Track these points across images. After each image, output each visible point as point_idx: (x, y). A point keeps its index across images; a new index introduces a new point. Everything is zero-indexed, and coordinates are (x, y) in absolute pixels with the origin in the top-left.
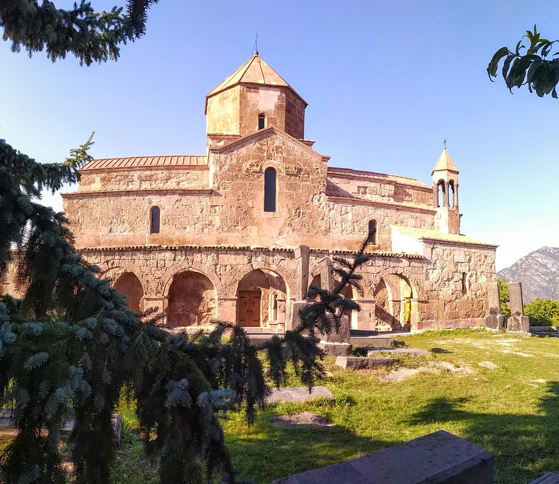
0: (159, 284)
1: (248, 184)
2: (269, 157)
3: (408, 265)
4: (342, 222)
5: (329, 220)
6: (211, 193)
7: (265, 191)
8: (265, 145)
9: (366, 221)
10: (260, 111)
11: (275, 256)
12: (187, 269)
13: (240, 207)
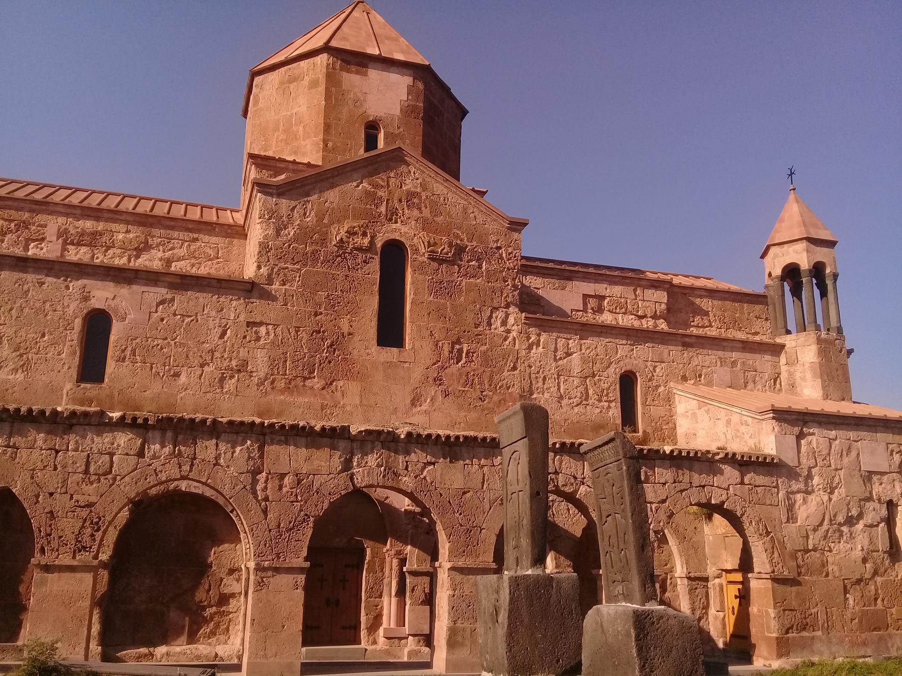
0: (87, 524)
1: (341, 278)
3: (739, 480)
4: (559, 376)
5: (528, 371)
9: (613, 374)
10: (368, 116)
12: (172, 487)
13: (319, 332)
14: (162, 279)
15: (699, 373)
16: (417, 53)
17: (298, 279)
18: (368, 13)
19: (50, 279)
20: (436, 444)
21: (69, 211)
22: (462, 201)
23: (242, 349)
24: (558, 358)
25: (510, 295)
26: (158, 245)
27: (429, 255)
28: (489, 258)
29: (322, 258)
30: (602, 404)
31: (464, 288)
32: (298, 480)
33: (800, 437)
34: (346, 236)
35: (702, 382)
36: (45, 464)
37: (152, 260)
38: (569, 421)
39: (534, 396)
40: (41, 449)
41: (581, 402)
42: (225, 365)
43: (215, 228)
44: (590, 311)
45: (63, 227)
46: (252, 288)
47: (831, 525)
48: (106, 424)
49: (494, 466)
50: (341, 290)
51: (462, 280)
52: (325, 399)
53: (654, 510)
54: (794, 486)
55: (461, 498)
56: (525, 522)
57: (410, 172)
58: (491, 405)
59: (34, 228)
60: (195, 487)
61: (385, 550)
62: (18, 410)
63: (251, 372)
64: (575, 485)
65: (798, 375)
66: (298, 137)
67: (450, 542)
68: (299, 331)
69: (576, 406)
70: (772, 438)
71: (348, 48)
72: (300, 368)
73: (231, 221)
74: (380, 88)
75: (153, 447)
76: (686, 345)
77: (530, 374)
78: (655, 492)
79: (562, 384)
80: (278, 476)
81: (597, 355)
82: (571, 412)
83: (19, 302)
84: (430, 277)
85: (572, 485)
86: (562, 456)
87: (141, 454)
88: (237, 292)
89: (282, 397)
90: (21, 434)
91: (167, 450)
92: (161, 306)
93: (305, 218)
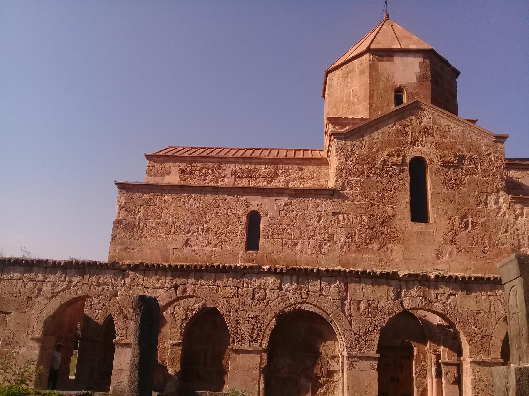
0: (255, 327)
1: (385, 183)
5: (516, 233)
7: (411, 191)
8: (408, 125)
11: (440, 289)
12: (297, 307)
13: (374, 216)
14: (285, 192)
16: (424, 43)
18: (391, 26)
19: (229, 197)
20: (455, 282)
21: (237, 160)
22: (461, 128)
23: (330, 228)
25: (499, 184)
28: (482, 162)
29: (373, 172)
31: (466, 182)
32: (369, 304)
36: (233, 295)
37: (279, 183)
39: (522, 249)
40: (231, 287)
42: (321, 238)
43: (311, 161)
45: (234, 169)
46: (334, 193)
49: (497, 296)
50: (386, 190)
51: (465, 177)
52: (380, 255)
55: (476, 317)
56: (524, 332)
58: (491, 257)
59: (220, 171)
60: (310, 308)
61: (426, 349)
62: (218, 266)
63: (336, 241)
66: (355, 104)
67: (470, 345)
68: (362, 216)
73: (320, 156)
74: (402, 68)
75: (286, 285)
77: (518, 234)
80: (357, 301)
84: (443, 177)
87: (280, 289)
88: (325, 196)
89: (355, 255)
90: (221, 279)
91: (294, 287)
92: (286, 207)
93: (361, 150)
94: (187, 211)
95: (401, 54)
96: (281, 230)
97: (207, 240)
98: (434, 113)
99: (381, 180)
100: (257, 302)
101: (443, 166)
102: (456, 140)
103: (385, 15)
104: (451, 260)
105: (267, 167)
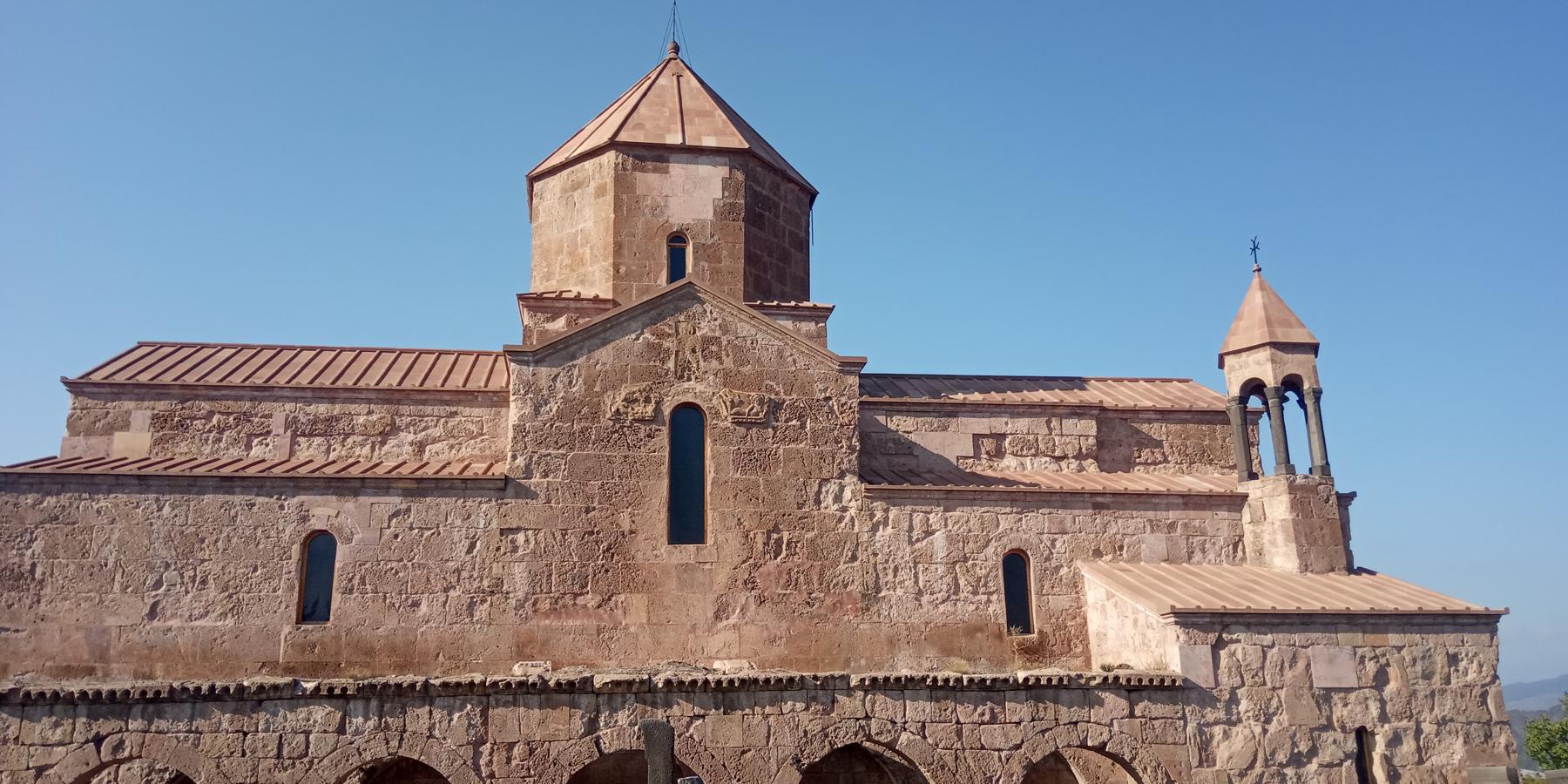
2: (683, 370)
3: (1126, 712)
4: (916, 564)
6: (504, 487)
8: (669, 335)
9: (992, 556)
10: (671, 226)
11: (675, 707)
13: (592, 533)
14: (394, 485)
15: (1119, 544)
17: (563, 467)
18: (678, 77)
19: (261, 499)
20: (705, 691)
21: (298, 394)
22: (776, 342)
23: (495, 565)
24: (913, 540)
25: (845, 461)
26: (407, 426)
27: (734, 418)
29: (593, 437)
30: (978, 597)
32: (530, 749)
33: (1217, 647)
34: (624, 406)
35: (1125, 556)
36: (233, 750)
37: (396, 454)
38: (932, 625)
39: (882, 594)
40: (227, 732)
41: (949, 597)
42: (475, 587)
44: (986, 456)
45: (292, 415)
46: (506, 485)
47: (1267, 766)
48: (300, 697)
49: (782, 714)
50: (619, 476)
51: (779, 447)
52: (601, 619)
53: (1003, 759)
54: (1209, 715)
57: (705, 311)
58: (823, 611)
59: (257, 420)
62: (198, 689)
63: (507, 593)
64: (893, 732)
65: (1266, 538)
68: (566, 534)
69: (941, 603)
70: (1176, 651)
71: (641, 139)
72: (569, 582)
74: (686, 187)
75: (354, 720)
76: (1098, 507)
77: (876, 564)
78: (1006, 735)
79: (920, 573)
81: (970, 531)
82: (934, 612)
83: (226, 530)
85: (890, 732)
86: (874, 695)
87: (341, 730)
88: (487, 492)
89: (547, 622)
90: (204, 716)
91: (371, 723)
92: (395, 520)
94: (155, 535)
95: (684, 156)
96: (383, 573)
97: (203, 603)
98: (724, 310)
99: (609, 454)
100: (287, 762)
101: (739, 423)
102: (765, 369)
103: (670, 46)
104: (744, 621)
105: (373, 411)
